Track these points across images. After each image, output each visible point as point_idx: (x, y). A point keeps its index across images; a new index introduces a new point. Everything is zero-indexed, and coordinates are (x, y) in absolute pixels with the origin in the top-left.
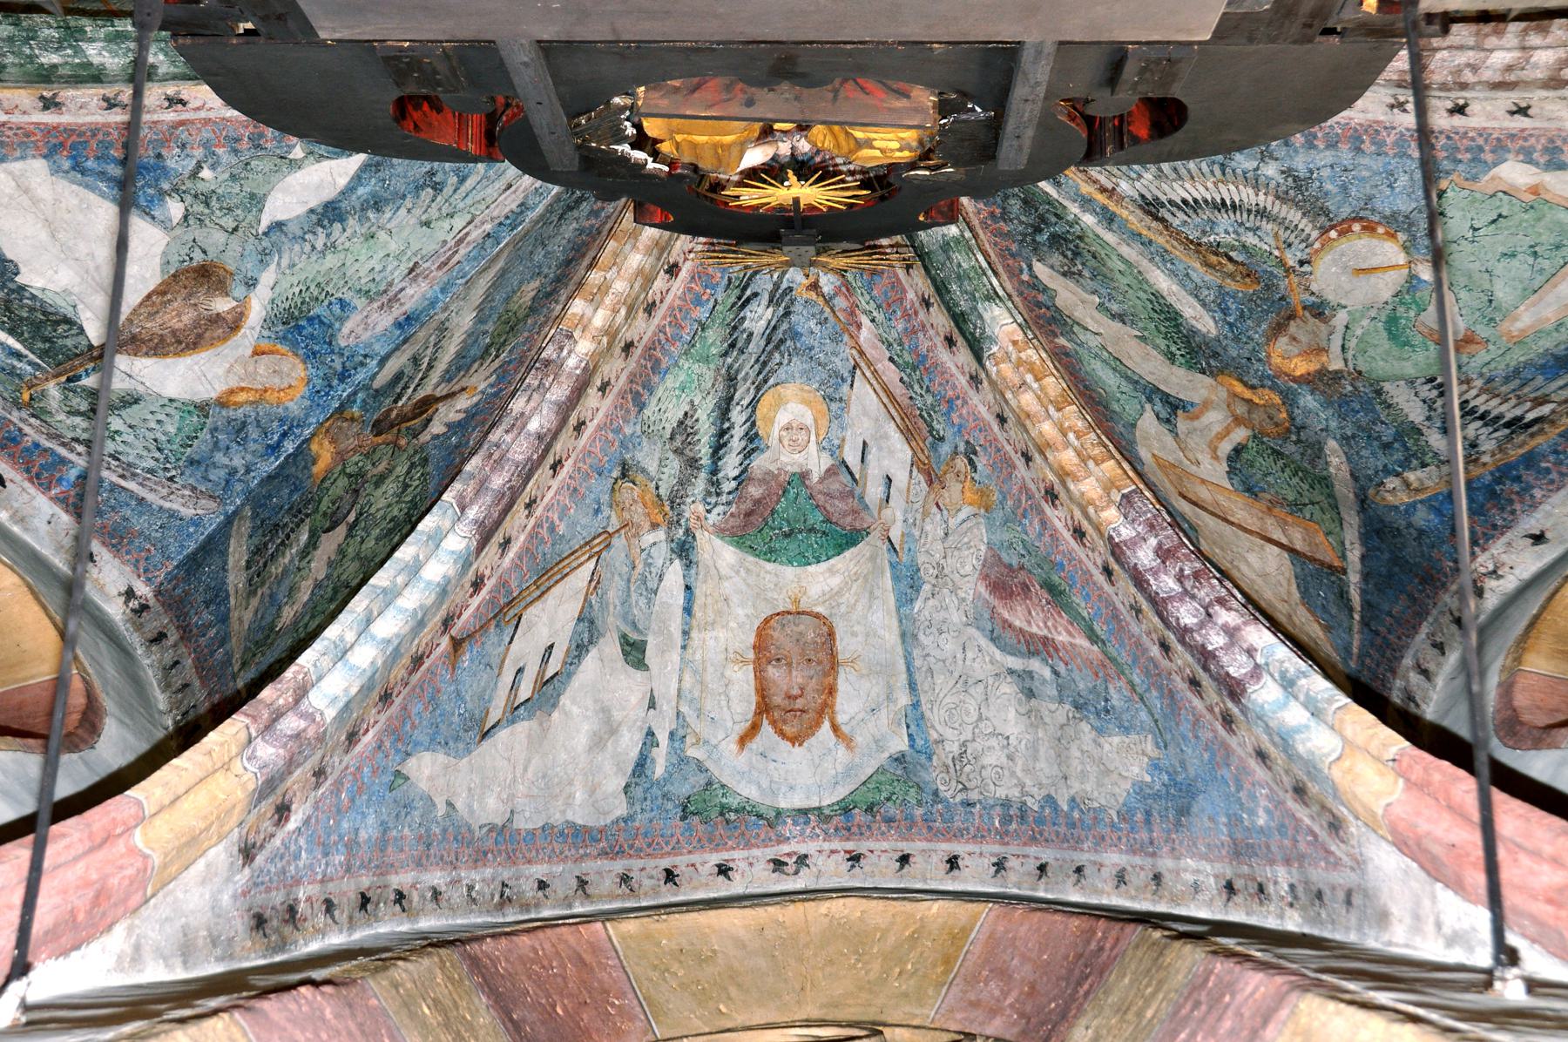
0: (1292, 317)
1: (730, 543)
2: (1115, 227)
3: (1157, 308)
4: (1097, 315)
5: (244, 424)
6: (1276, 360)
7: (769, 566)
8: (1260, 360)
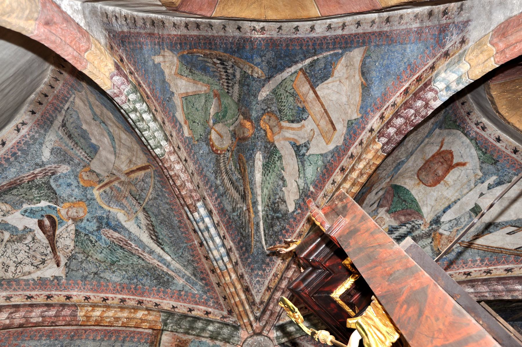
0: (240, 139)
1: (422, 212)
2: (255, 200)
3: (267, 172)
4: (289, 185)
6: (251, 131)
7: (417, 198)
8: (255, 135)
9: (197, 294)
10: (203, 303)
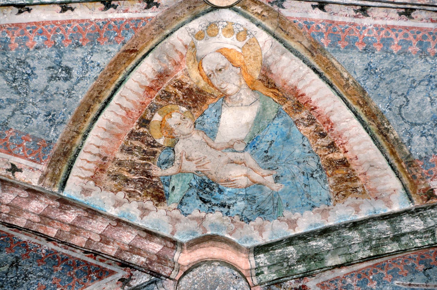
9: (392, 280)
10: (366, 274)
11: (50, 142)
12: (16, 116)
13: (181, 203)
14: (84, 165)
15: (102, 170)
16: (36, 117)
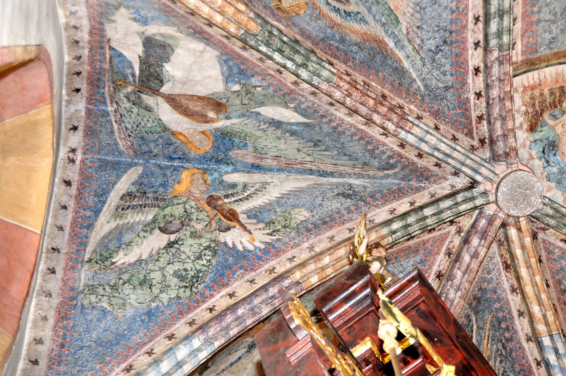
5: (172, 144)
11: (537, 51)
12: (546, 24)
13: (535, 141)
14: (531, 78)
15: (532, 89)
16: (550, 34)
